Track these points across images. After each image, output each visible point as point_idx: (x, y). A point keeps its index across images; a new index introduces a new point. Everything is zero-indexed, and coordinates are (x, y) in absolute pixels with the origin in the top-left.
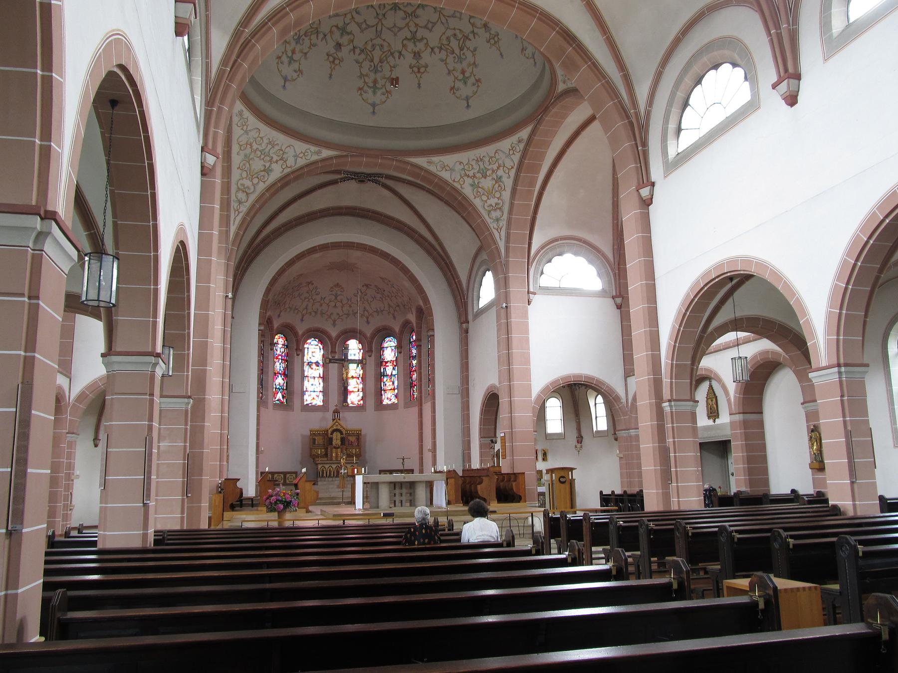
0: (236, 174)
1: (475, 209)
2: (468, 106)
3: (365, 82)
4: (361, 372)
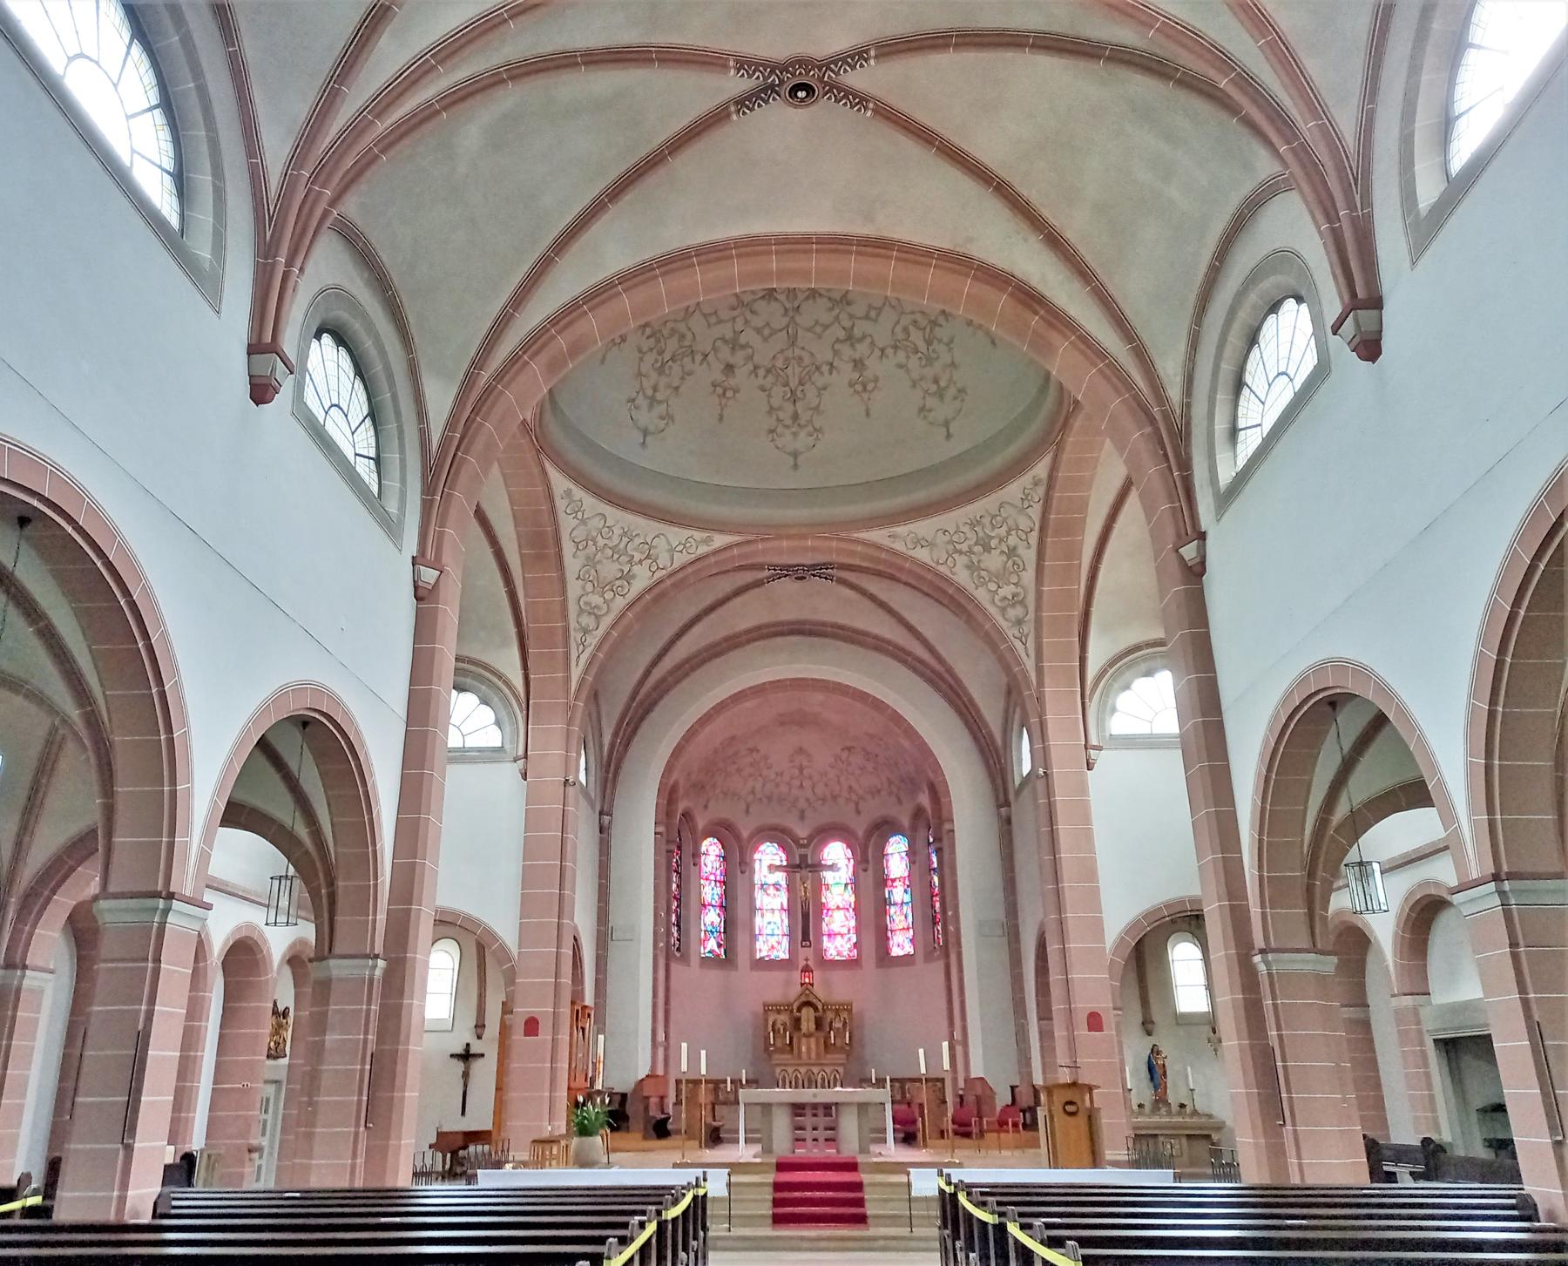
0: (574, 588)
1: (979, 607)
2: (949, 436)
3: (778, 420)
4: (852, 899)
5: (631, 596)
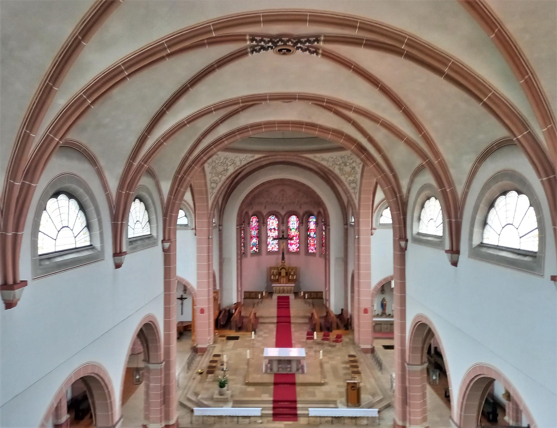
0: (209, 176)
1: (341, 181)
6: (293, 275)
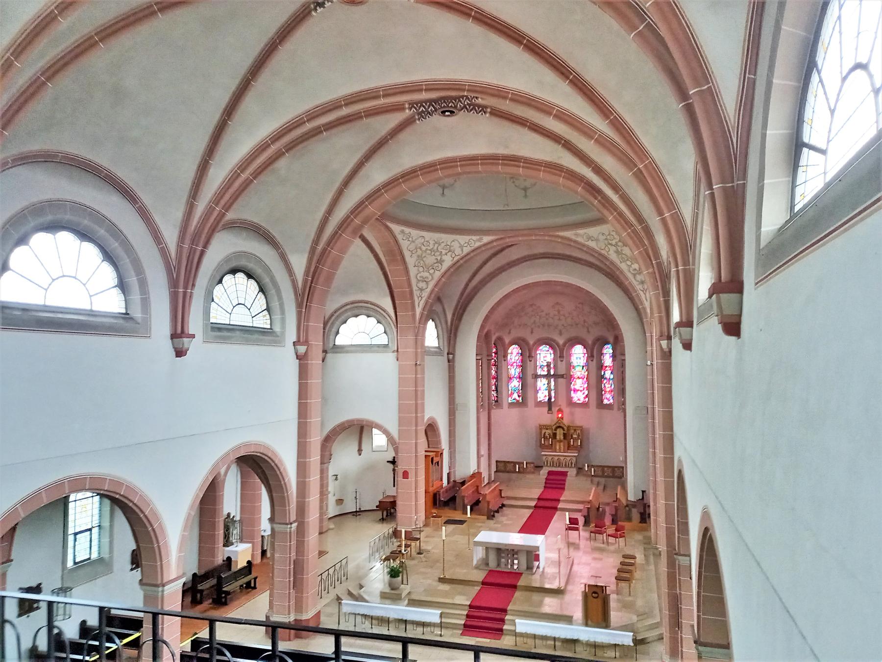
0: (413, 271)
5: (443, 270)
6: (575, 440)
